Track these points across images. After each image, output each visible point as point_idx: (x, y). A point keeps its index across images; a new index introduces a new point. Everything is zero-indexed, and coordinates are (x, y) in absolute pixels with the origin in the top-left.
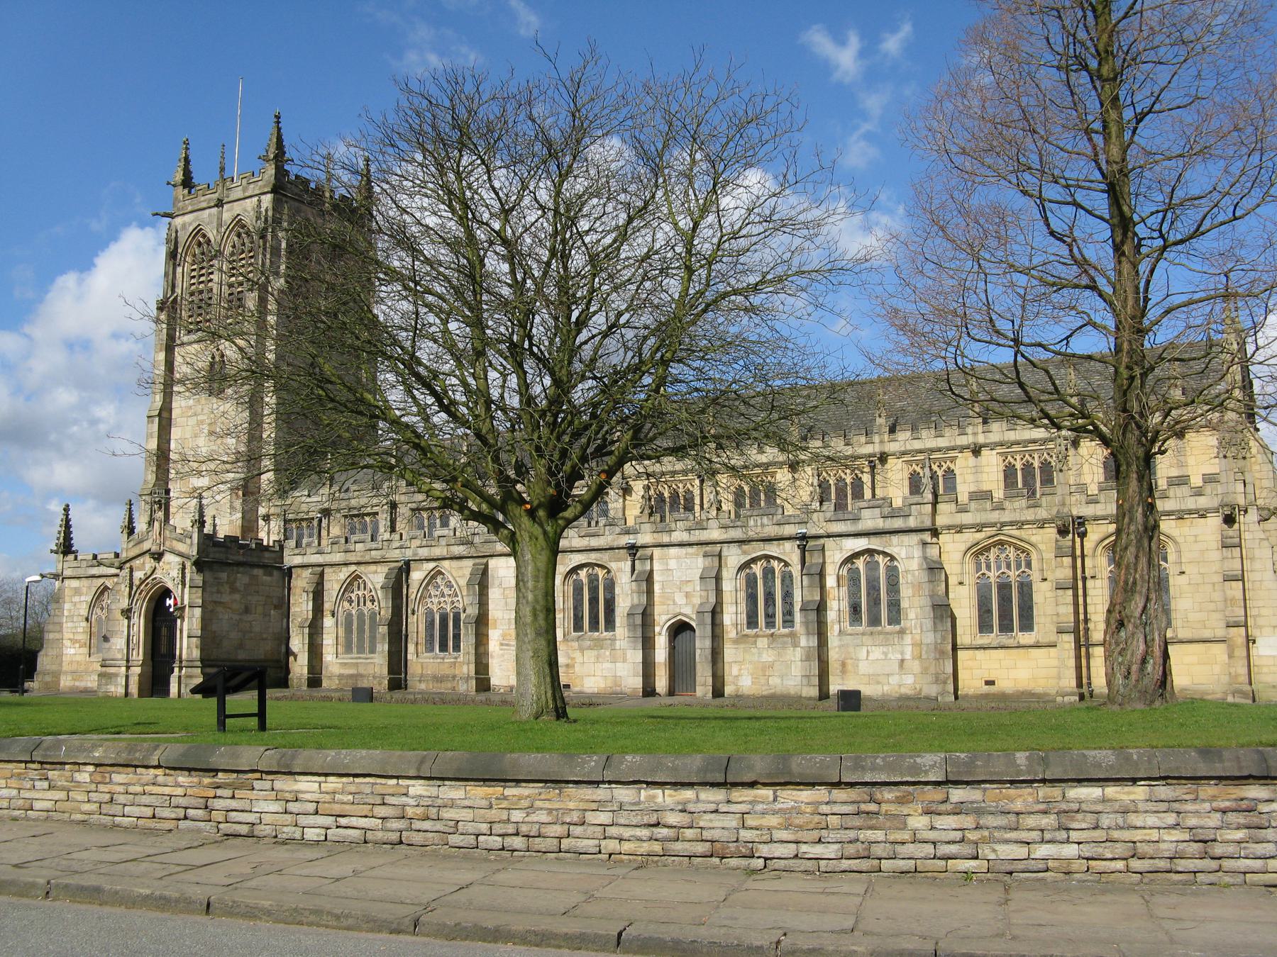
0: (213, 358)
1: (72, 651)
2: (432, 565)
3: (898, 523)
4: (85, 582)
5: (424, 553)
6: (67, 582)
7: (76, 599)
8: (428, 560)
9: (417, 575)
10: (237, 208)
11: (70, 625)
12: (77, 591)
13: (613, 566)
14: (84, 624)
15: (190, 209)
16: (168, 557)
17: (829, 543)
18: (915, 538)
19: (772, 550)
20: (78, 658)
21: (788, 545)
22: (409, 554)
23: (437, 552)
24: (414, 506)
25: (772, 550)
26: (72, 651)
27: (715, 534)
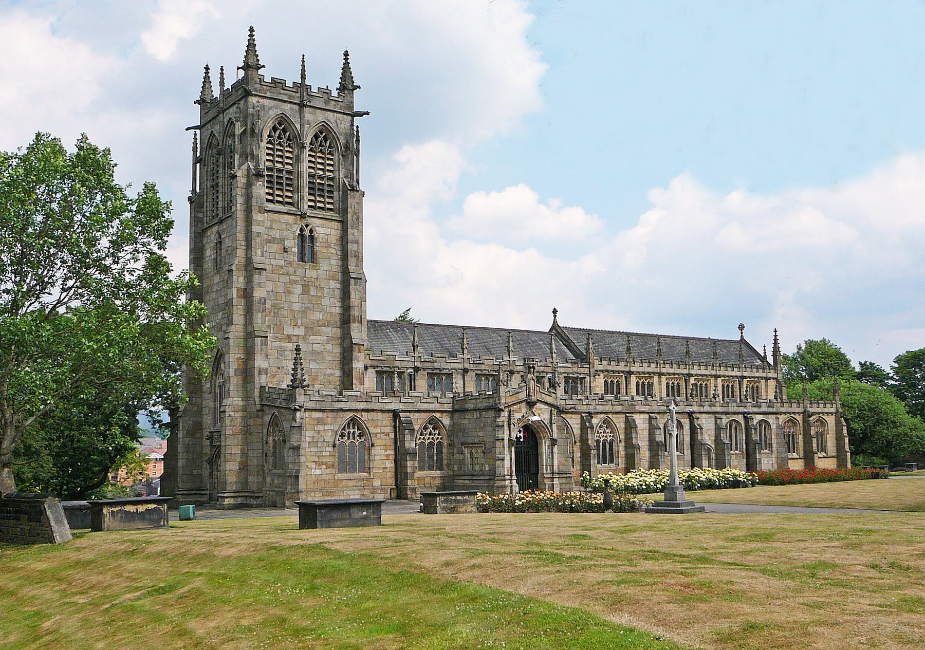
0: (301, 230)
1: (318, 472)
2: (602, 416)
3: (771, 410)
4: (330, 414)
5: (600, 409)
6: (307, 414)
7: (320, 427)
8: (601, 413)
9: (595, 421)
10: (320, 116)
11: (313, 449)
12: (319, 421)
13: (682, 420)
14: (331, 449)
15: (268, 95)
16: (538, 405)
17: (753, 416)
18: (774, 416)
19: (736, 417)
20: (324, 477)
21: (741, 416)
22: (591, 409)
23: (608, 408)
24: (479, 372)
25: (736, 417)
26: (318, 472)
27: (719, 409)
